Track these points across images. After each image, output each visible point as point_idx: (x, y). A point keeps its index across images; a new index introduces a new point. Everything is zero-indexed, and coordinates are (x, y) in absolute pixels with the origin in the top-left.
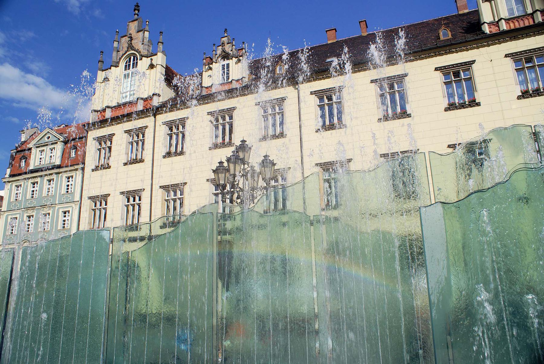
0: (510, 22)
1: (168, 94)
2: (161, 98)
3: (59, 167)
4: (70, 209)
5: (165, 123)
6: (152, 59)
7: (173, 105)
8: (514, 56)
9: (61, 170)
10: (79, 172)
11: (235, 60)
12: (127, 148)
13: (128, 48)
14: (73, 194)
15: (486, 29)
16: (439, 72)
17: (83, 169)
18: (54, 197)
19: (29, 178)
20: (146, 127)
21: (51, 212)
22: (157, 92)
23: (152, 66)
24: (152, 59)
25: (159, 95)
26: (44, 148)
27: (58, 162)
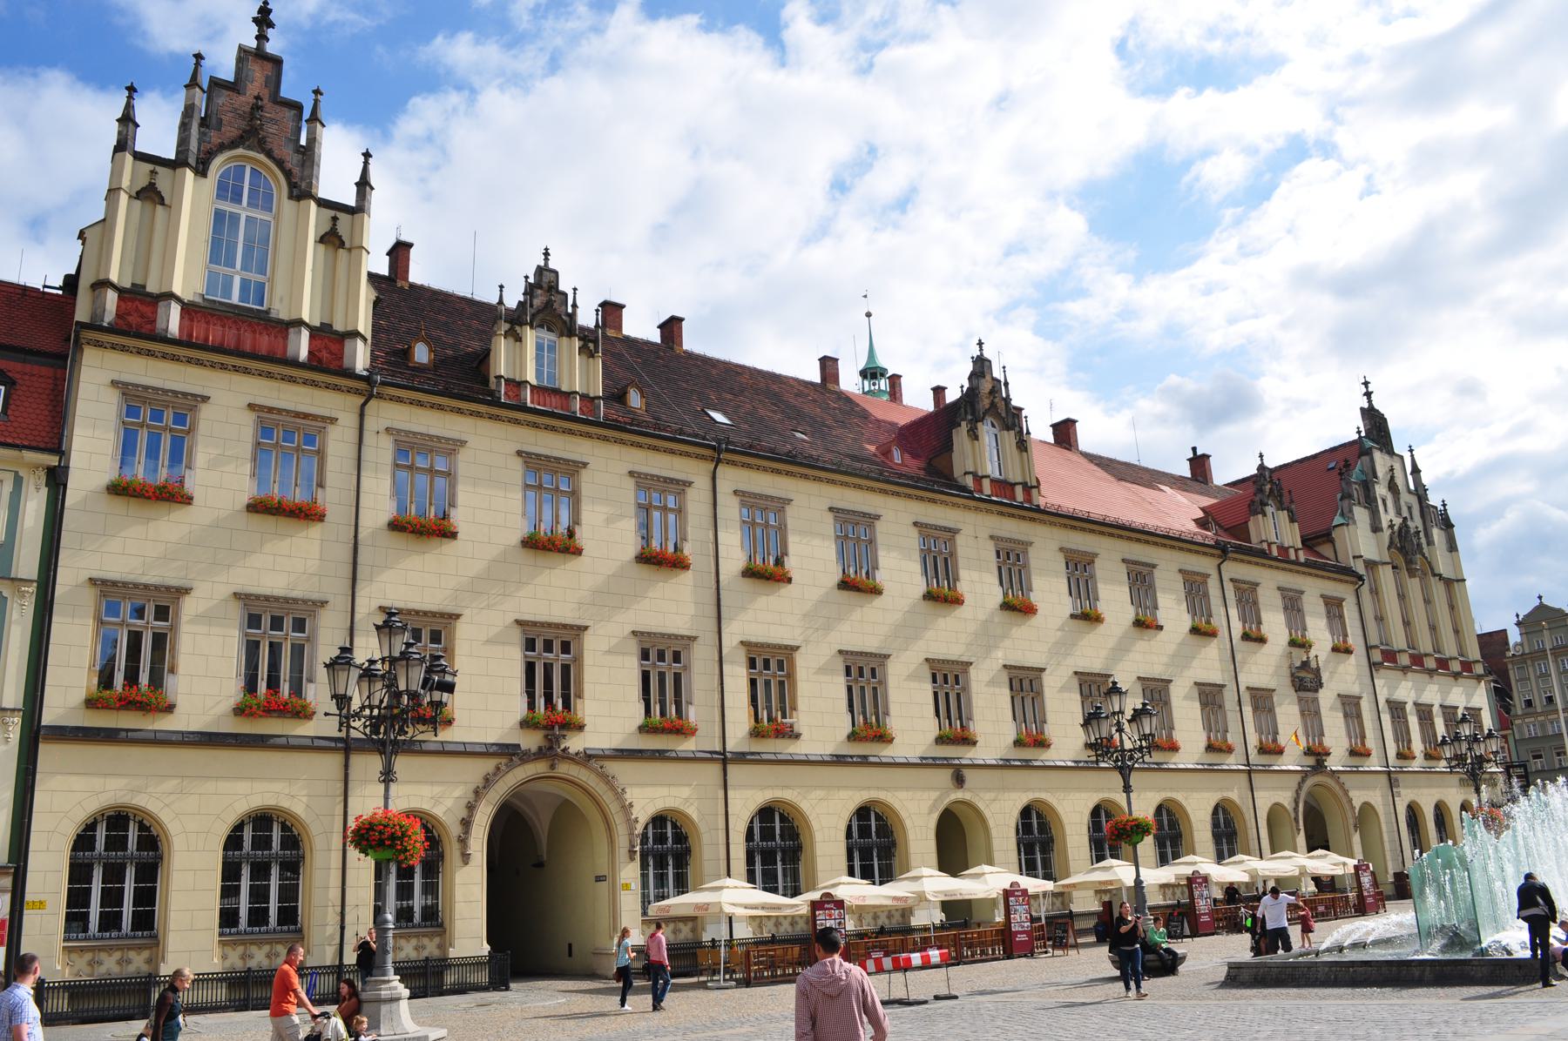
24: (335, 219)
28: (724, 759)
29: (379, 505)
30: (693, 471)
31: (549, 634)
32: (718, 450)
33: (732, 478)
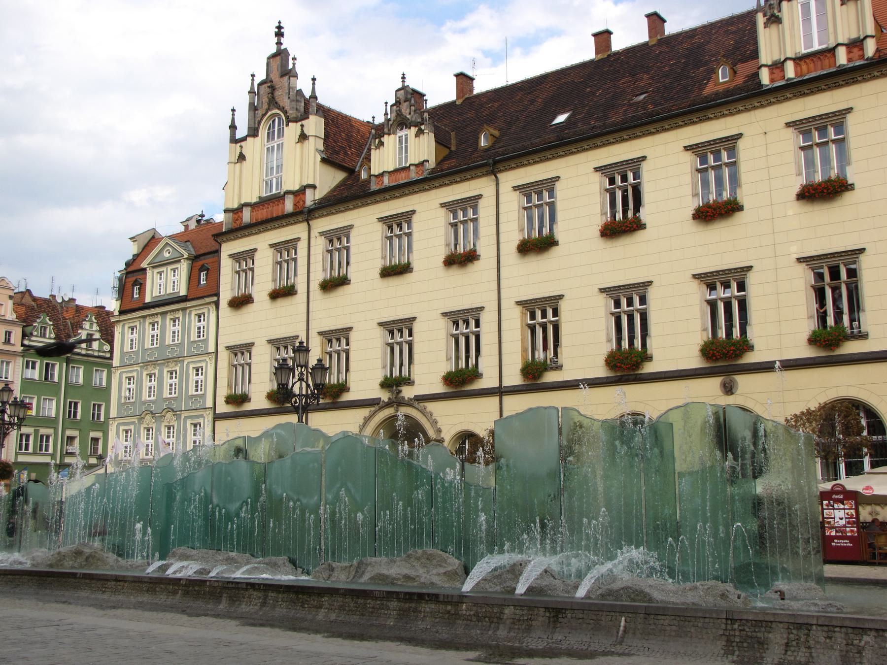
0: (802, 63)
1: (327, 180)
2: (317, 191)
3: (184, 299)
4: (203, 364)
5: (322, 234)
6: (302, 126)
7: (336, 201)
8: (800, 126)
9: (189, 304)
10: (212, 308)
11: (414, 130)
12: (274, 271)
13: (269, 105)
14: (206, 341)
15: (765, 77)
16: (689, 153)
17: (217, 304)
18: (180, 345)
19: (144, 317)
20: (298, 239)
21: (178, 369)
22: (311, 182)
23: (303, 137)
24: (302, 126)
25: (314, 187)
26: (164, 269)
27: (183, 292)
28: (500, 392)
29: (512, 237)
30: (481, 186)
31: (399, 326)
32: (493, 164)
33: (511, 178)
